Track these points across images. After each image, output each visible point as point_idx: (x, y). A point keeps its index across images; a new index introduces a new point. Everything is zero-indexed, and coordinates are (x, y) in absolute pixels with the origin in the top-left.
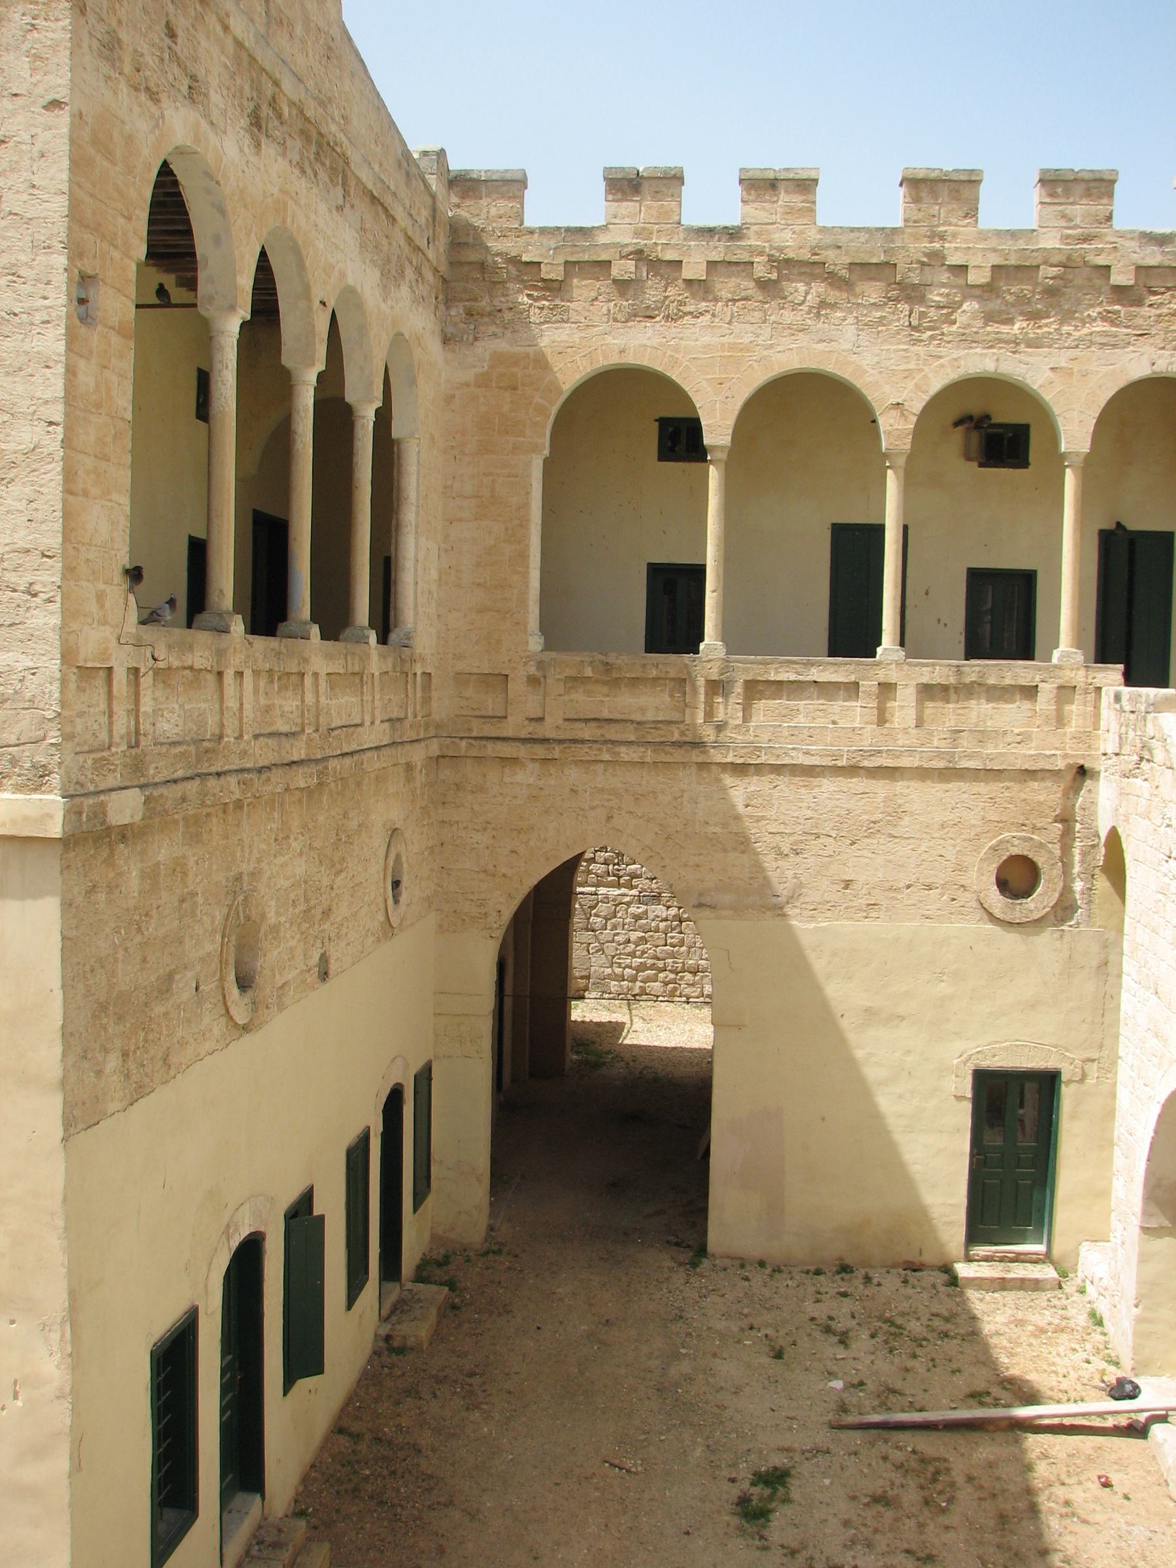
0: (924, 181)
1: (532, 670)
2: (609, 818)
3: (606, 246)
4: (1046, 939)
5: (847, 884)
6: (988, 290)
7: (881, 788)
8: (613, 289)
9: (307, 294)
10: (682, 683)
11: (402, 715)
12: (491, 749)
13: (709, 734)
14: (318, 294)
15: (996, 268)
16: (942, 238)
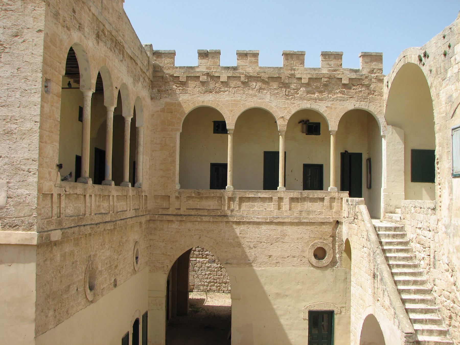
0: (289, 54)
1: (177, 194)
2: (200, 238)
3: (198, 72)
4: (328, 272)
5: (270, 256)
6: (308, 85)
7: (279, 228)
8: (200, 84)
9: (112, 85)
10: (221, 198)
11: (139, 208)
12: (165, 218)
13: (229, 213)
14: (115, 85)
16: (294, 70)
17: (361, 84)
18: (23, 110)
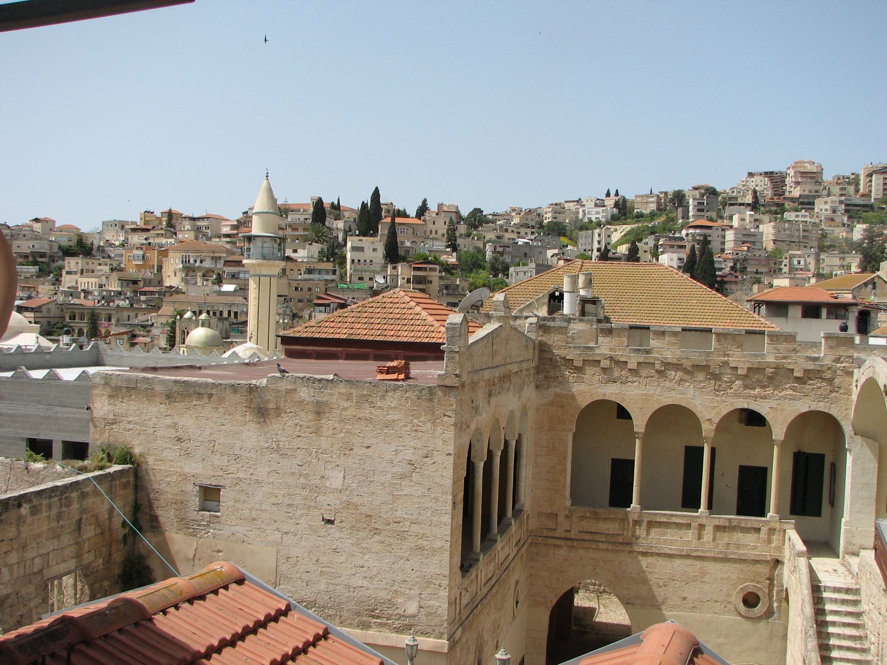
1: (567, 512)
3: (599, 354)
4: (762, 625)
5: (684, 599)
6: (745, 377)
7: (698, 564)
10: (624, 520)
12: (550, 541)
15: (749, 369)
17: (821, 378)
18: (434, 529)
